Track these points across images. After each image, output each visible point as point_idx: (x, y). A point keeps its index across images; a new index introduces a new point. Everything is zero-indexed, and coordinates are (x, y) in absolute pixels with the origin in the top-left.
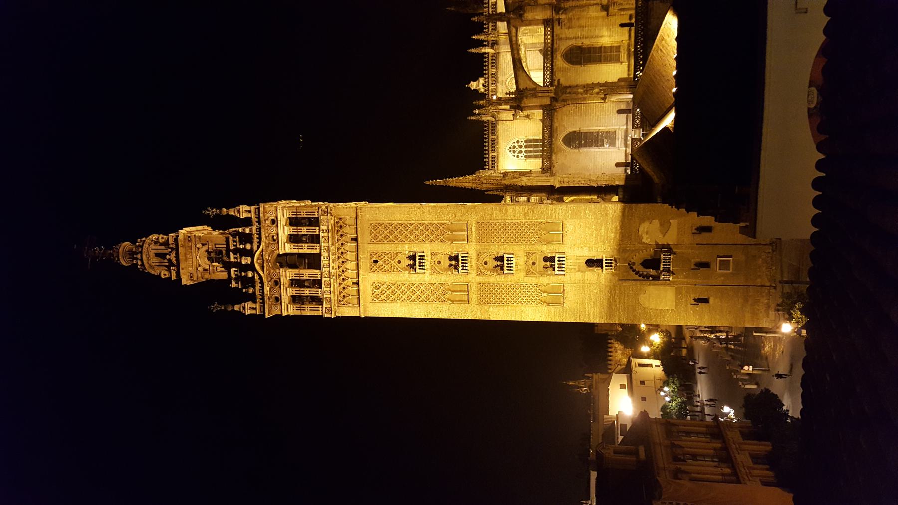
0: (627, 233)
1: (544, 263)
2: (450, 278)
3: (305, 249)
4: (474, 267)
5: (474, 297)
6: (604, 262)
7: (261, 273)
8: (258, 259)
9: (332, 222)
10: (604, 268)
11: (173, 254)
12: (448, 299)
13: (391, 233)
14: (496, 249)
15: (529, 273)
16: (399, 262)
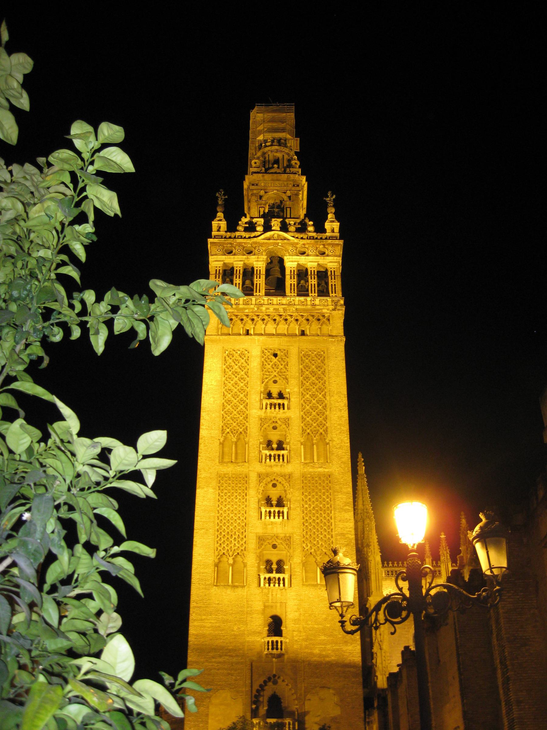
0: (319, 672)
1: (274, 560)
2: (255, 438)
3: (290, 281)
4: (269, 470)
5: (229, 469)
6: (278, 639)
7: (262, 237)
8: (279, 235)
9: (325, 311)
10: (270, 639)
11: (278, 171)
12: (225, 438)
13: (313, 373)
14: (294, 497)
15: (261, 540)
16: (275, 382)
